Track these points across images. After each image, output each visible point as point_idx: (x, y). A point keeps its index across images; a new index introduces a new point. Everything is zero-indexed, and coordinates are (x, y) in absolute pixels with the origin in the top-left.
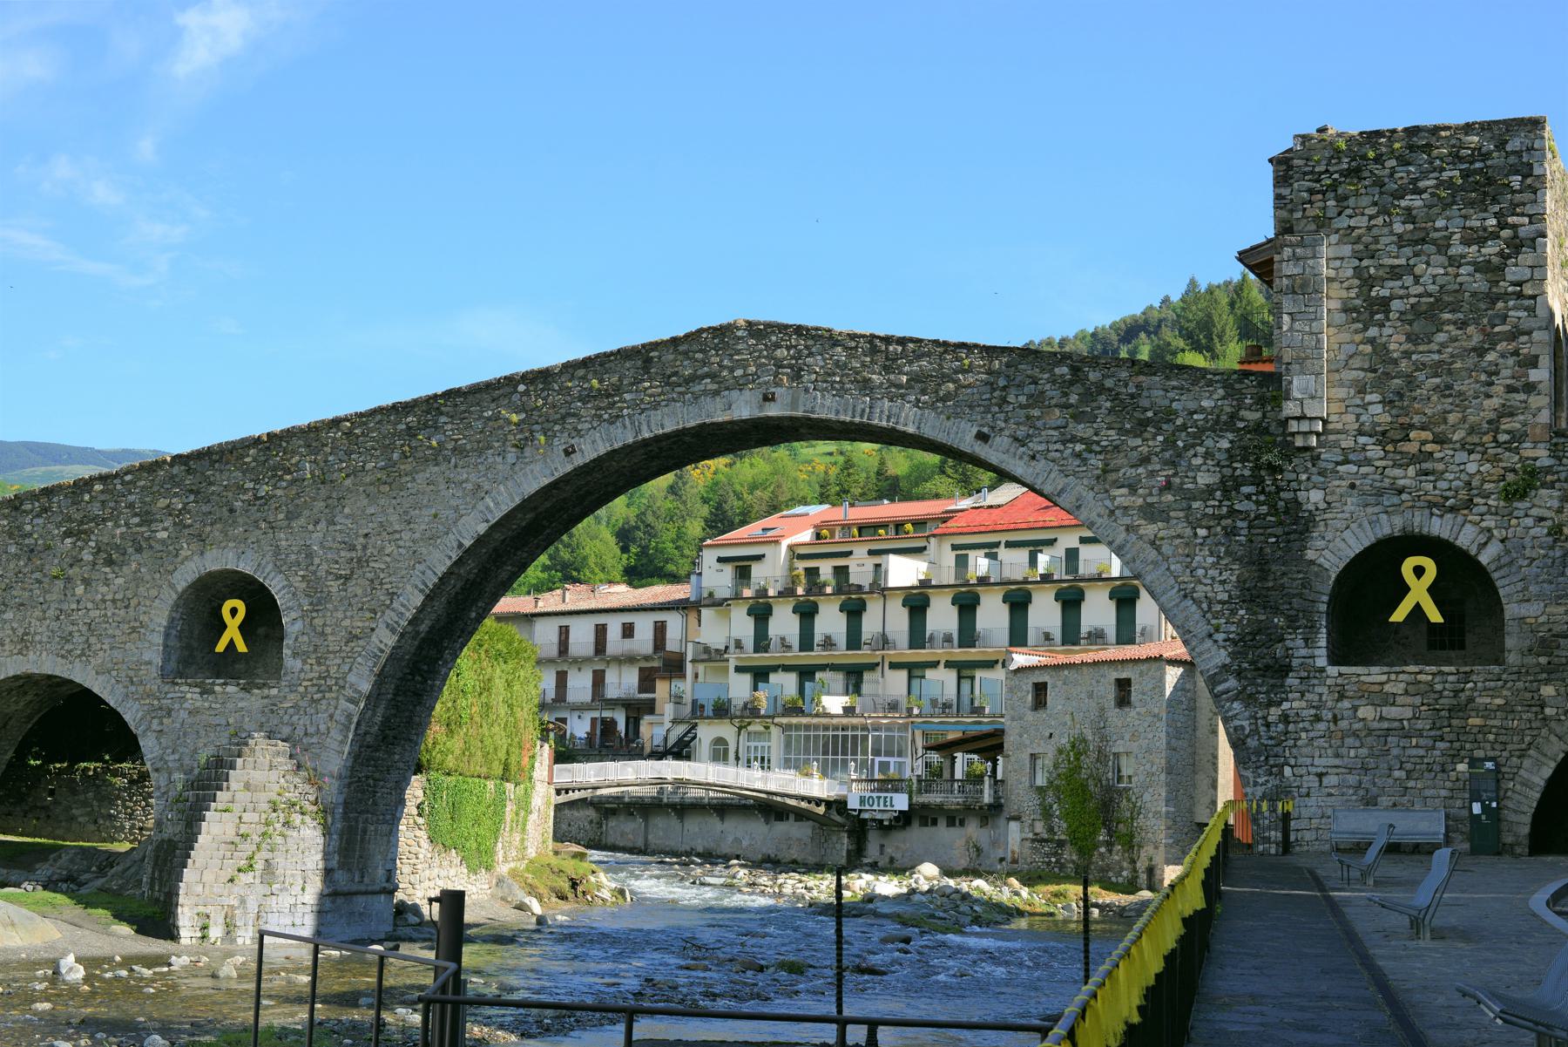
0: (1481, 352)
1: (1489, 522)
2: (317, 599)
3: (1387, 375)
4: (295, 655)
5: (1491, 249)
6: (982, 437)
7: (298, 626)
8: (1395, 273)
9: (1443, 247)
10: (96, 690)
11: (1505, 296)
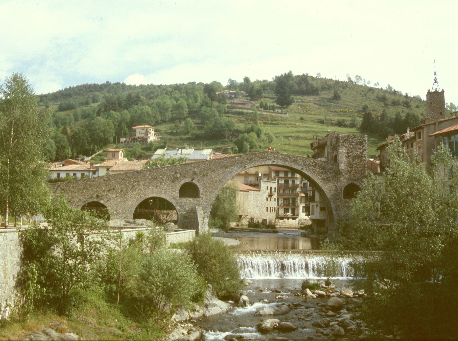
0: (360, 163)
1: (360, 182)
2: (205, 186)
3: (350, 165)
4: (202, 195)
5: (362, 150)
6: (302, 169)
7: (202, 190)
8: (351, 152)
9: (356, 149)
10: (168, 199)
11: (363, 156)
